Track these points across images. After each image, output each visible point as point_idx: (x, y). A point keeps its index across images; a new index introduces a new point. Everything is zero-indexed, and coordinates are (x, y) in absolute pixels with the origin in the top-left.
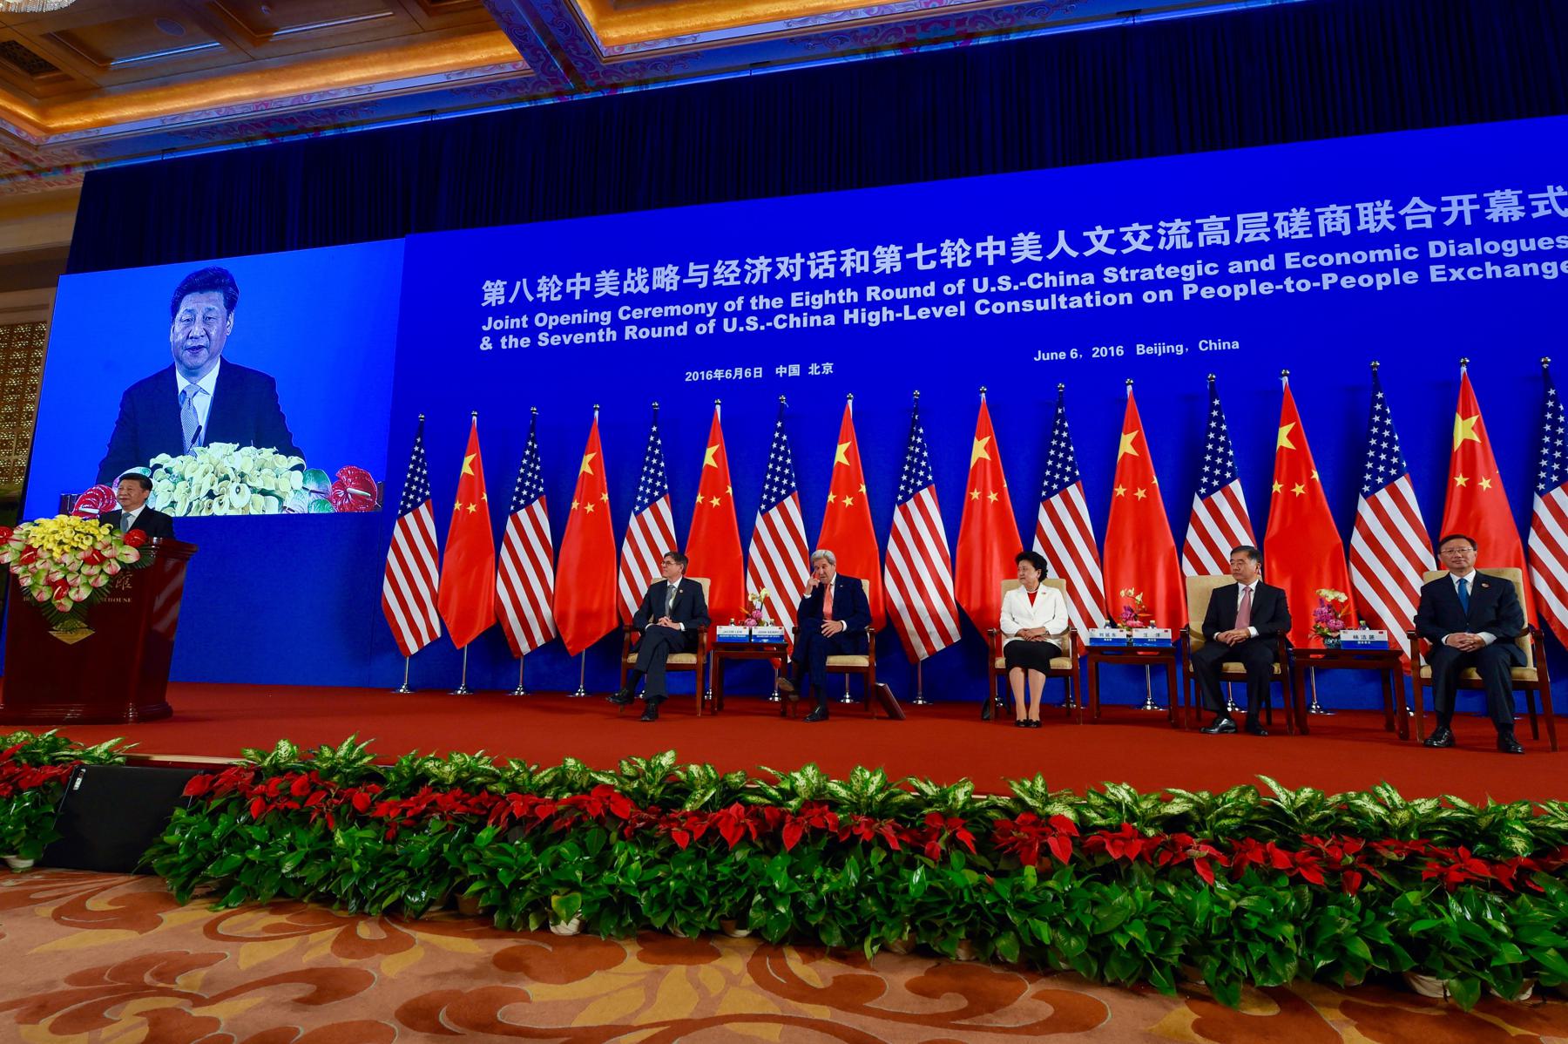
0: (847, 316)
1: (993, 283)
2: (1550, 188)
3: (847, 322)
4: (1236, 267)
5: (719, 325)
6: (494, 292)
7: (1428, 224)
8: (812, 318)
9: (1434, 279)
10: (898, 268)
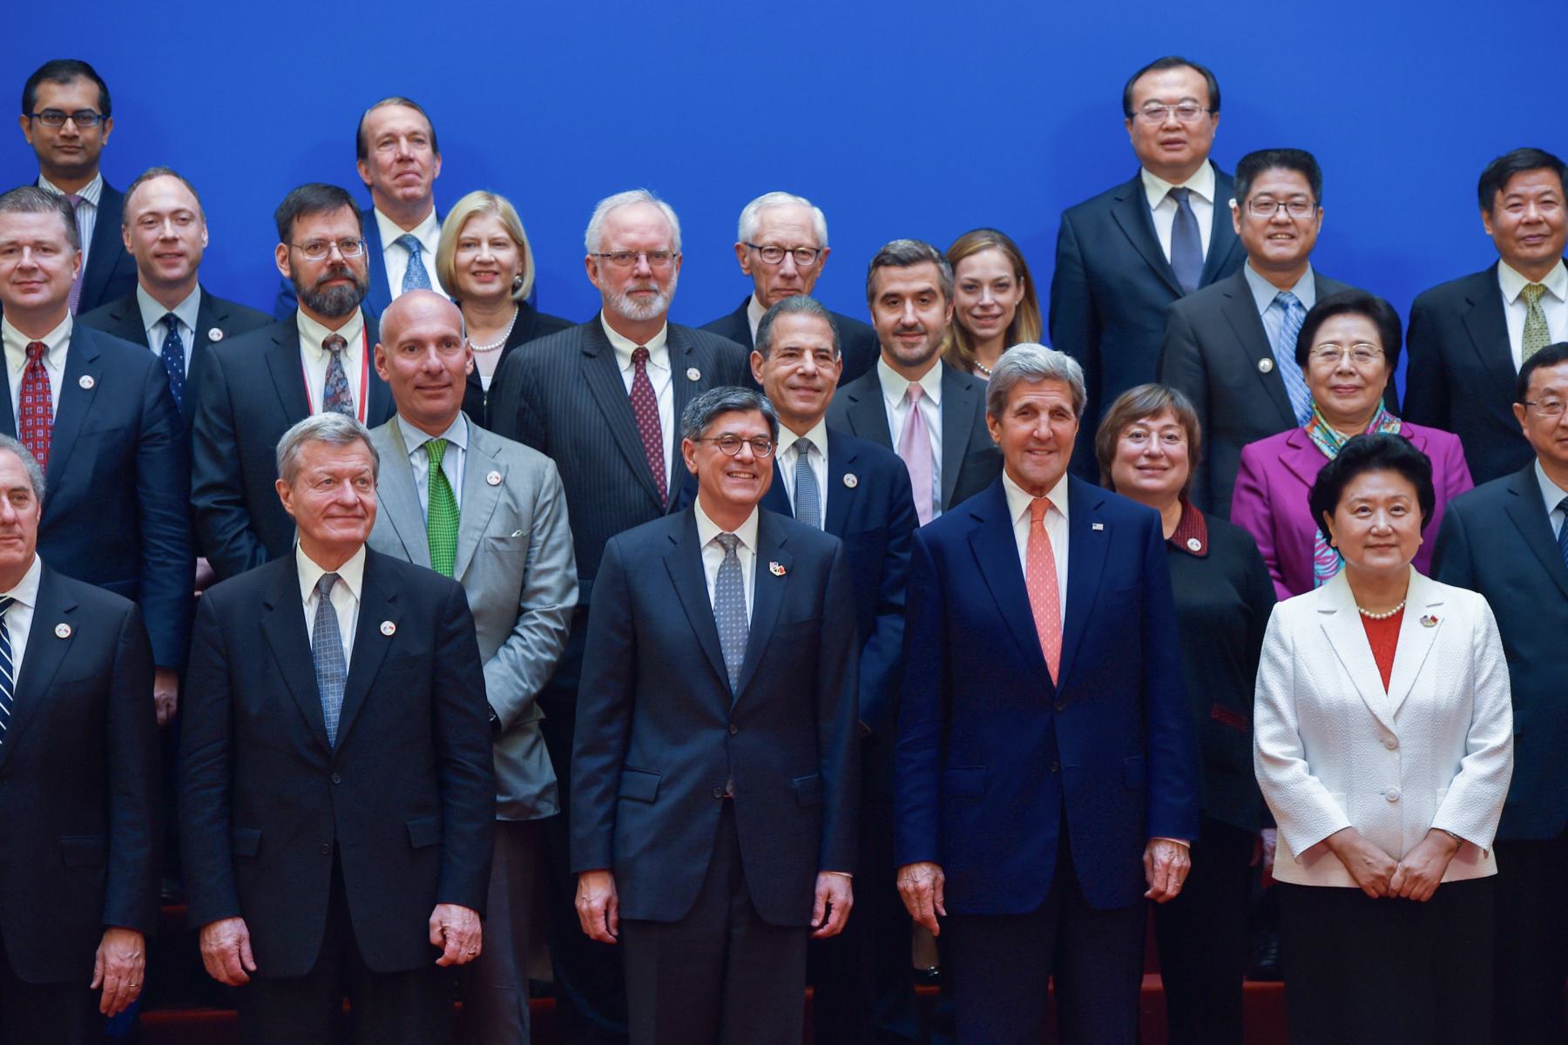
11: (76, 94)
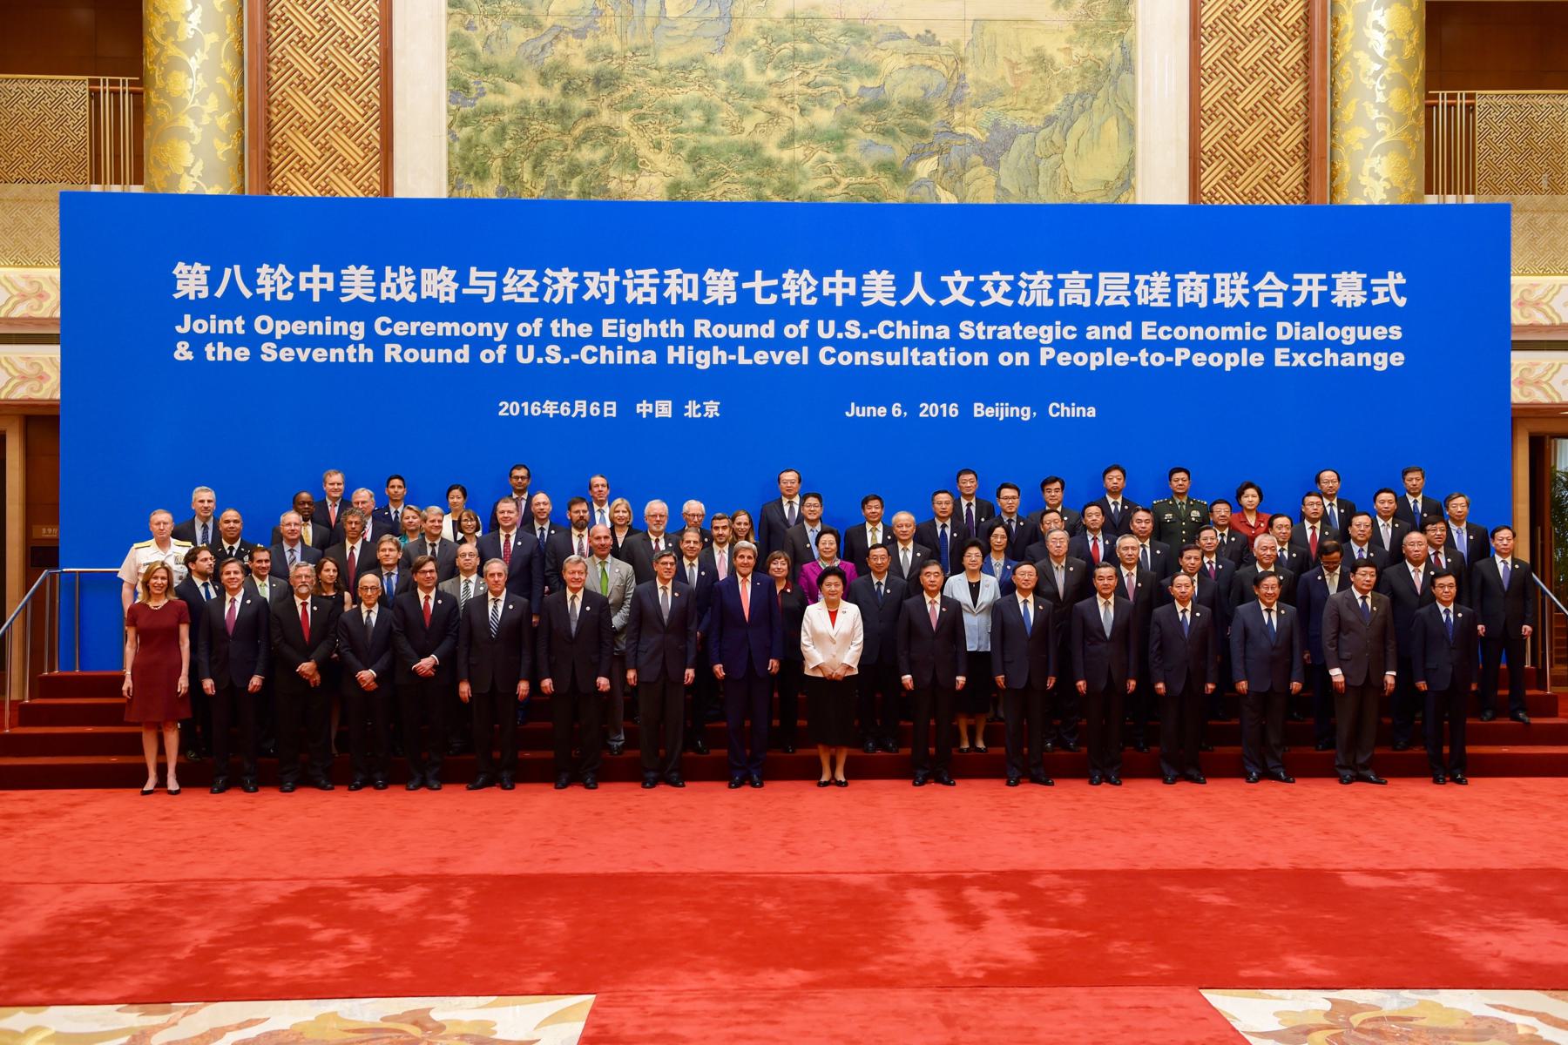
0: (671, 354)
1: (840, 328)
2: (1391, 273)
3: (671, 361)
4: (1093, 332)
5: (511, 354)
6: (191, 280)
7: (1279, 304)
8: (629, 354)
9: (1278, 363)
10: (733, 300)
11: (522, 472)
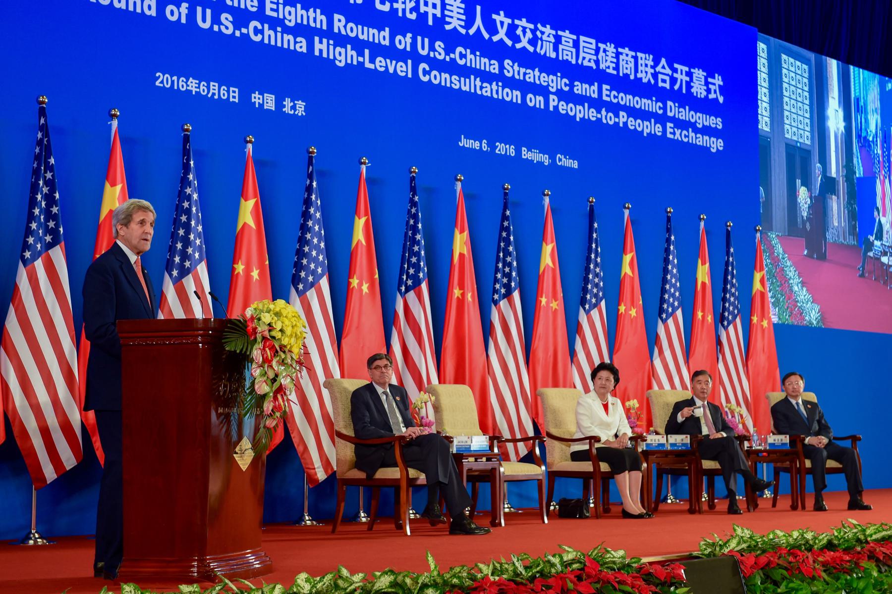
4: (580, 88)
